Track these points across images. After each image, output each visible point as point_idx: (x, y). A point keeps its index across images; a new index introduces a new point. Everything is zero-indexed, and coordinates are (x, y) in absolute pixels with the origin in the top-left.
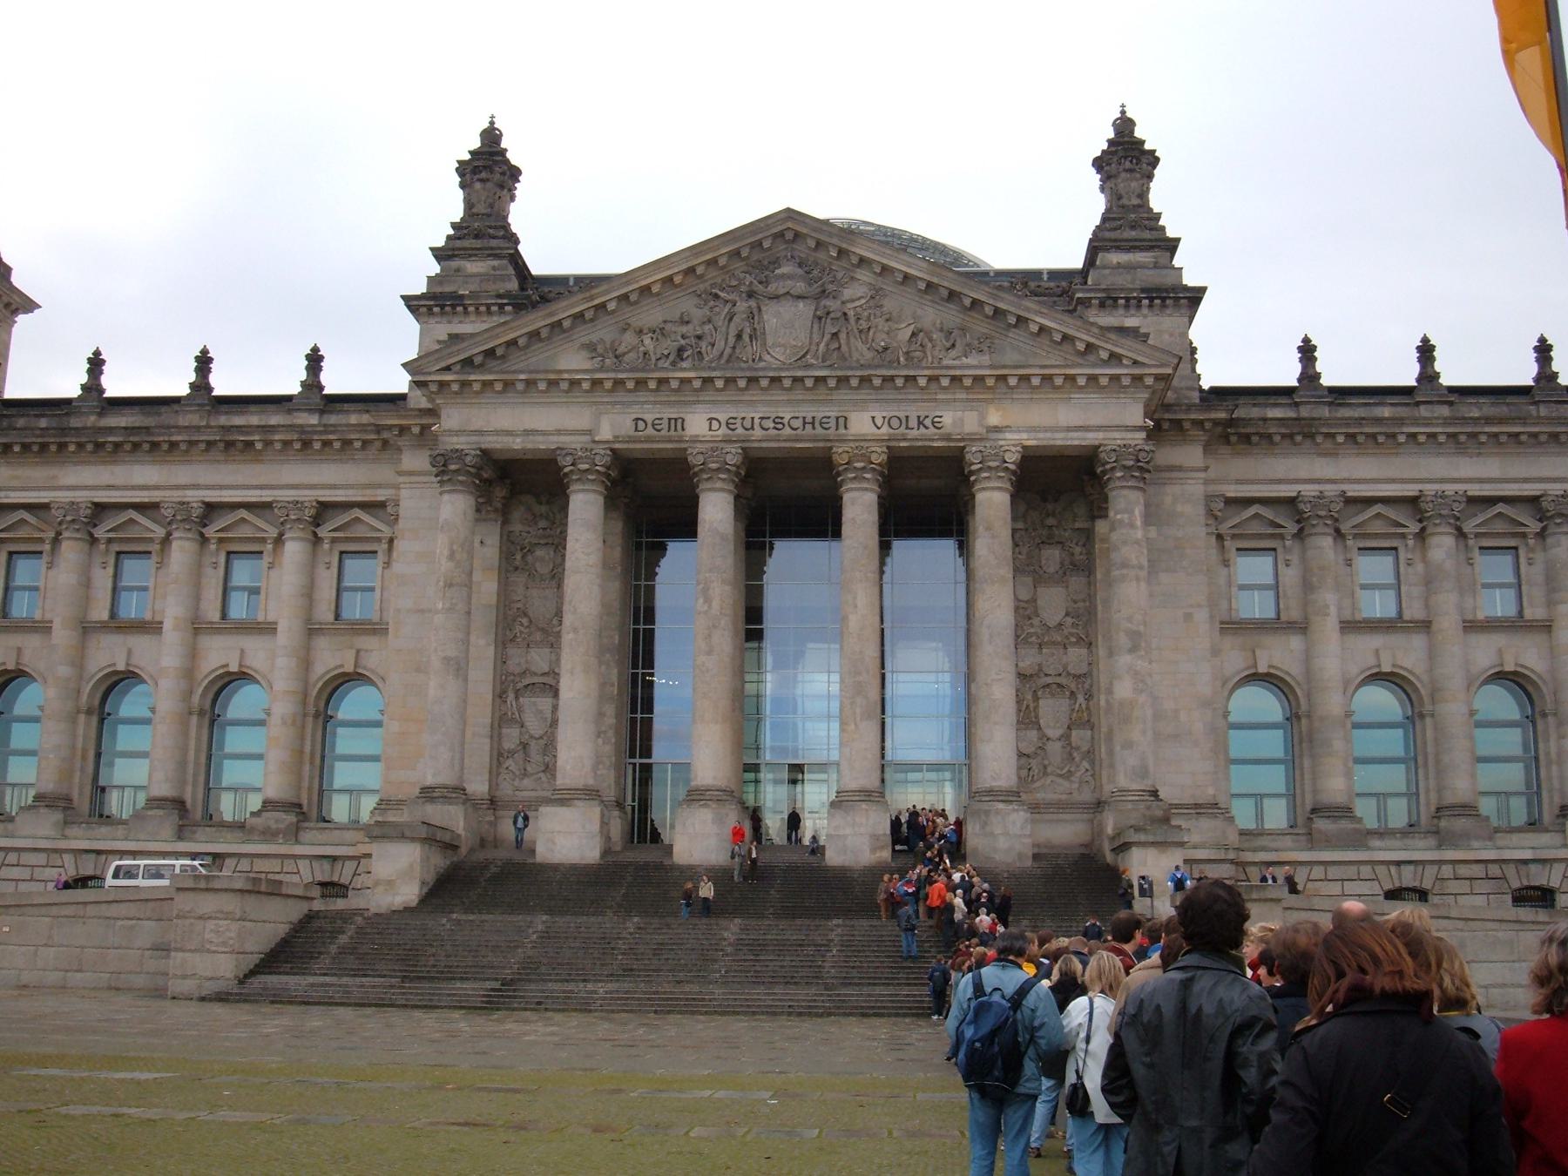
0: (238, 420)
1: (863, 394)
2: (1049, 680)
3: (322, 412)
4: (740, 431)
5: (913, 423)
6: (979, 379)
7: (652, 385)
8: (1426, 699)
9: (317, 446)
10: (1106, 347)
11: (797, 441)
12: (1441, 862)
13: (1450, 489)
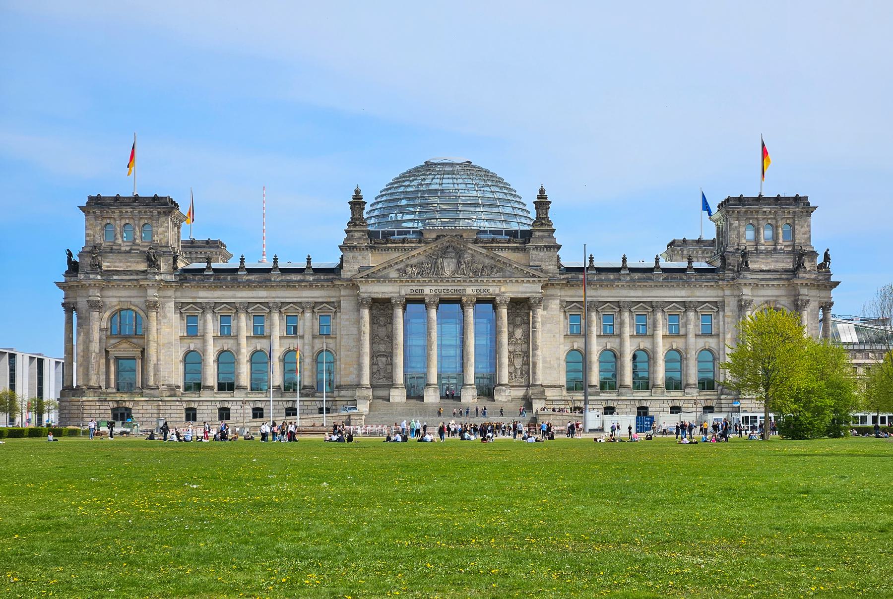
0: (288, 278)
1: (470, 284)
2: (517, 353)
3: (312, 275)
4: (438, 293)
5: (482, 291)
6: (499, 281)
7: (416, 282)
8: (619, 356)
9: (314, 287)
10: (532, 272)
11: (452, 295)
12: (619, 400)
13: (628, 299)
